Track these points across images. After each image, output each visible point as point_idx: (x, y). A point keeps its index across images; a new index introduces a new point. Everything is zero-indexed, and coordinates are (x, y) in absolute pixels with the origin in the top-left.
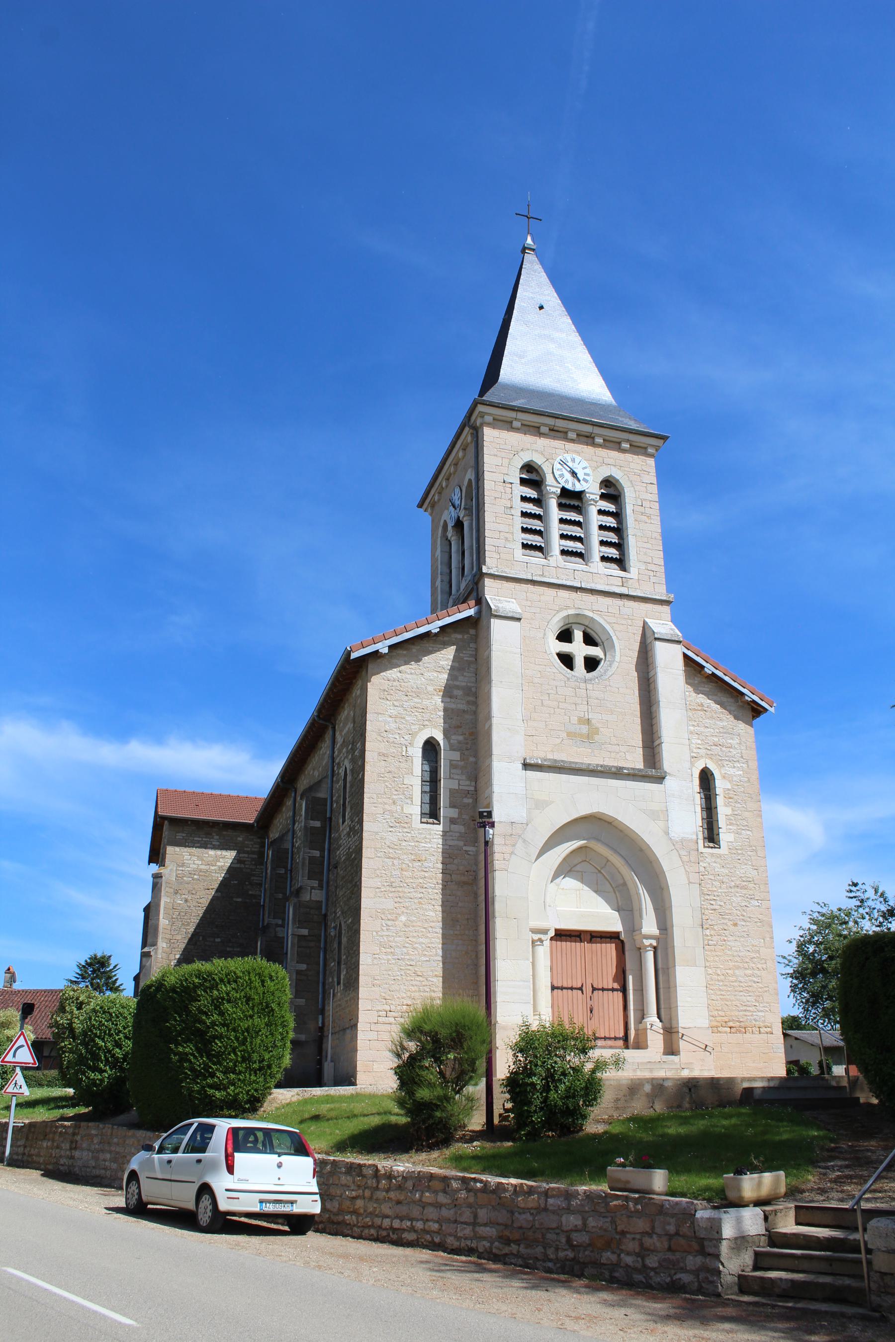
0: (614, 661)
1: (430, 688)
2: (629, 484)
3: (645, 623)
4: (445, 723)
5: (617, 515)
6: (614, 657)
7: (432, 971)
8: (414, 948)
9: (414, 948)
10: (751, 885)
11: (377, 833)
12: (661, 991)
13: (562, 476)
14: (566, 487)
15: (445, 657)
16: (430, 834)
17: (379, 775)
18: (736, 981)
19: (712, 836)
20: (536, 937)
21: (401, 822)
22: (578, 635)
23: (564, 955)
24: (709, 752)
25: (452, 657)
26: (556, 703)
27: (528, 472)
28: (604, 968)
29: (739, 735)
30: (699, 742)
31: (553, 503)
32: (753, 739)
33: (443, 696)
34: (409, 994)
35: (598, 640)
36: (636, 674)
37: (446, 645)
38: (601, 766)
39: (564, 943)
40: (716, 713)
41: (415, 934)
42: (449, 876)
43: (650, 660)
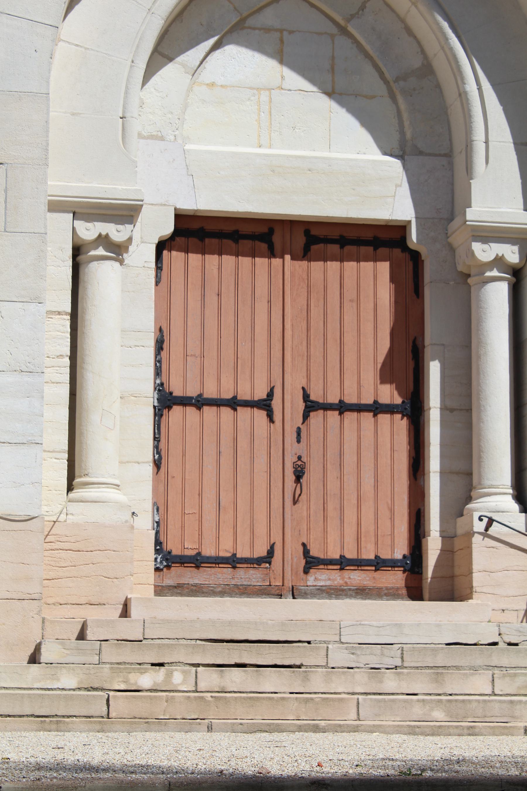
20: (88, 231)
23: (212, 299)
28: (350, 338)
39: (212, 260)
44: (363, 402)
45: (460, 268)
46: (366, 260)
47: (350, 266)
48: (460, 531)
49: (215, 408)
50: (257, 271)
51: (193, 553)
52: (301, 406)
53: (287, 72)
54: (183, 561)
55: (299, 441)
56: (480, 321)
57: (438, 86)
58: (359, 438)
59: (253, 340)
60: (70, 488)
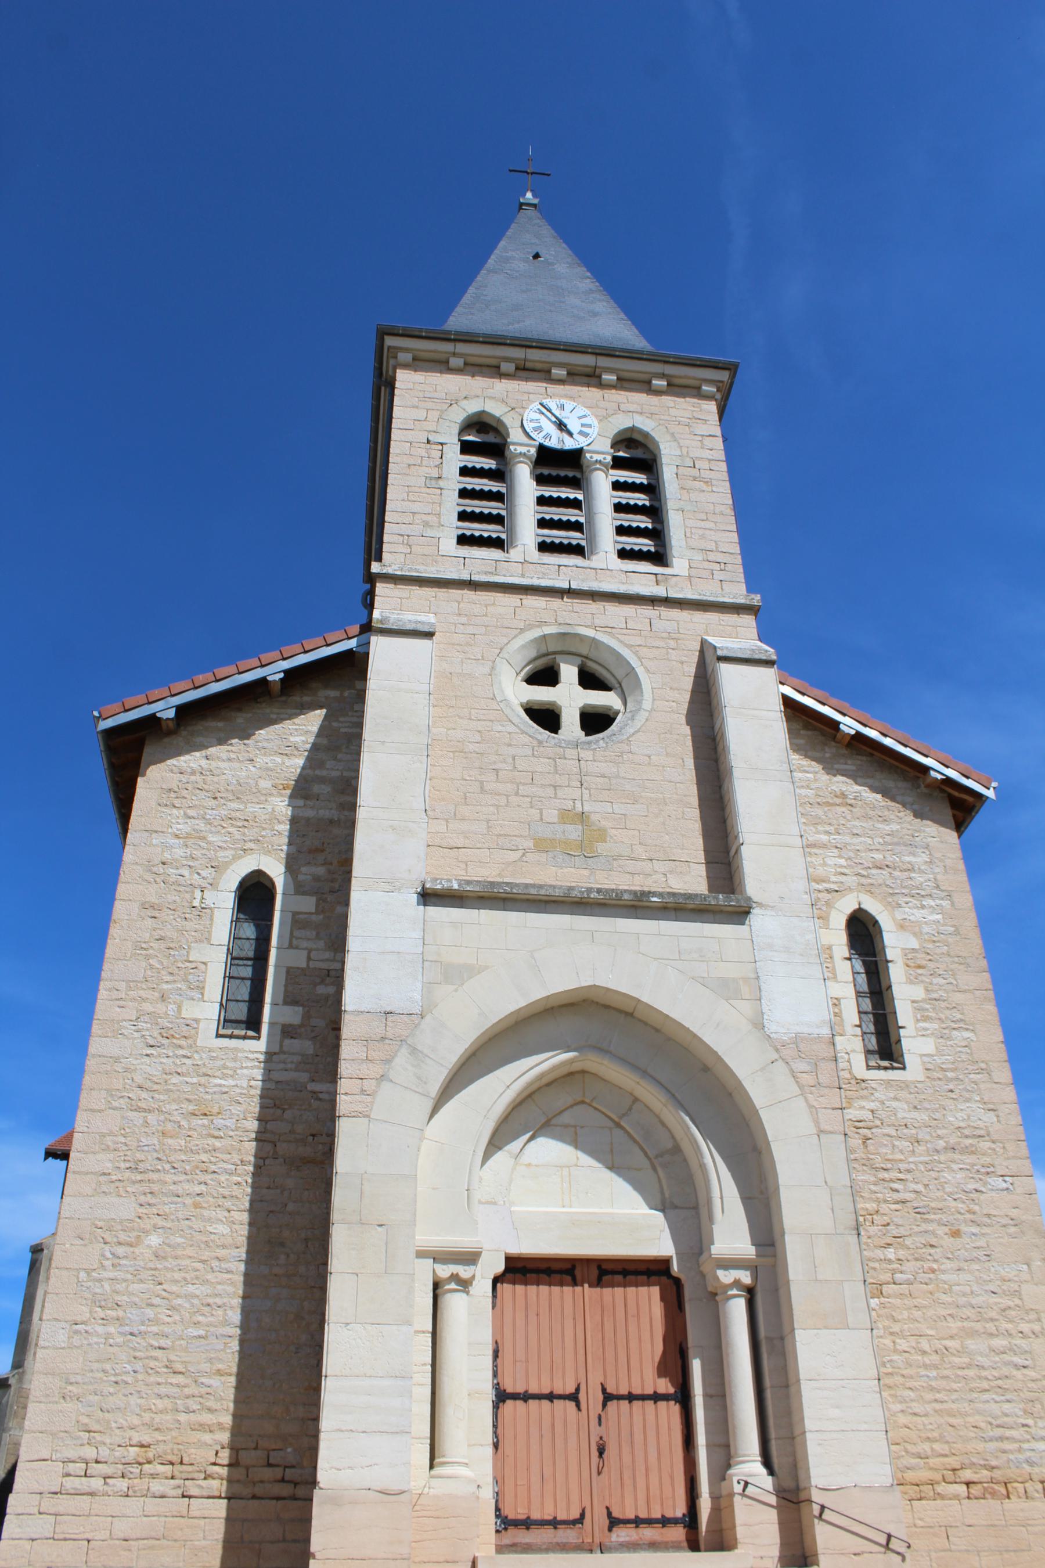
0: (639, 709)
1: (265, 784)
2: (668, 437)
3: (703, 642)
4: (290, 844)
5: (652, 489)
6: (640, 702)
7: (210, 1360)
8: (173, 1308)
9: (173, 1308)
10: (985, 1145)
11: (117, 1060)
12: (768, 1394)
13: (539, 429)
14: (547, 443)
15: (304, 728)
16: (235, 1060)
17: (138, 946)
18: (969, 1366)
19: (886, 1048)
20: (444, 1271)
21: (176, 1035)
22: (569, 672)
24: (864, 881)
25: (315, 729)
26: (510, 788)
27: (479, 432)
28: (634, 1345)
29: (927, 847)
30: (843, 862)
31: (523, 476)
32: (959, 854)
33: (292, 797)
34: (147, 1416)
35: (611, 681)
36: (687, 730)
37: (304, 708)
38: (599, 891)
39: (532, 1289)
40: (874, 808)
41: (177, 1276)
42: (269, 1147)
43: (714, 703)
44: (646, 1392)
45: (710, 1289)
46: (643, 1285)
47: (631, 1290)
48: (724, 1492)
49: (537, 1401)
50: (565, 1295)
51: (524, 1517)
52: (601, 1397)
53: (580, 1154)
54: (516, 1523)
55: (600, 1425)
56: (727, 1328)
57: (685, 1160)
58: (644, 1420)
59: (563, 1348)
60: (431, 1467)
